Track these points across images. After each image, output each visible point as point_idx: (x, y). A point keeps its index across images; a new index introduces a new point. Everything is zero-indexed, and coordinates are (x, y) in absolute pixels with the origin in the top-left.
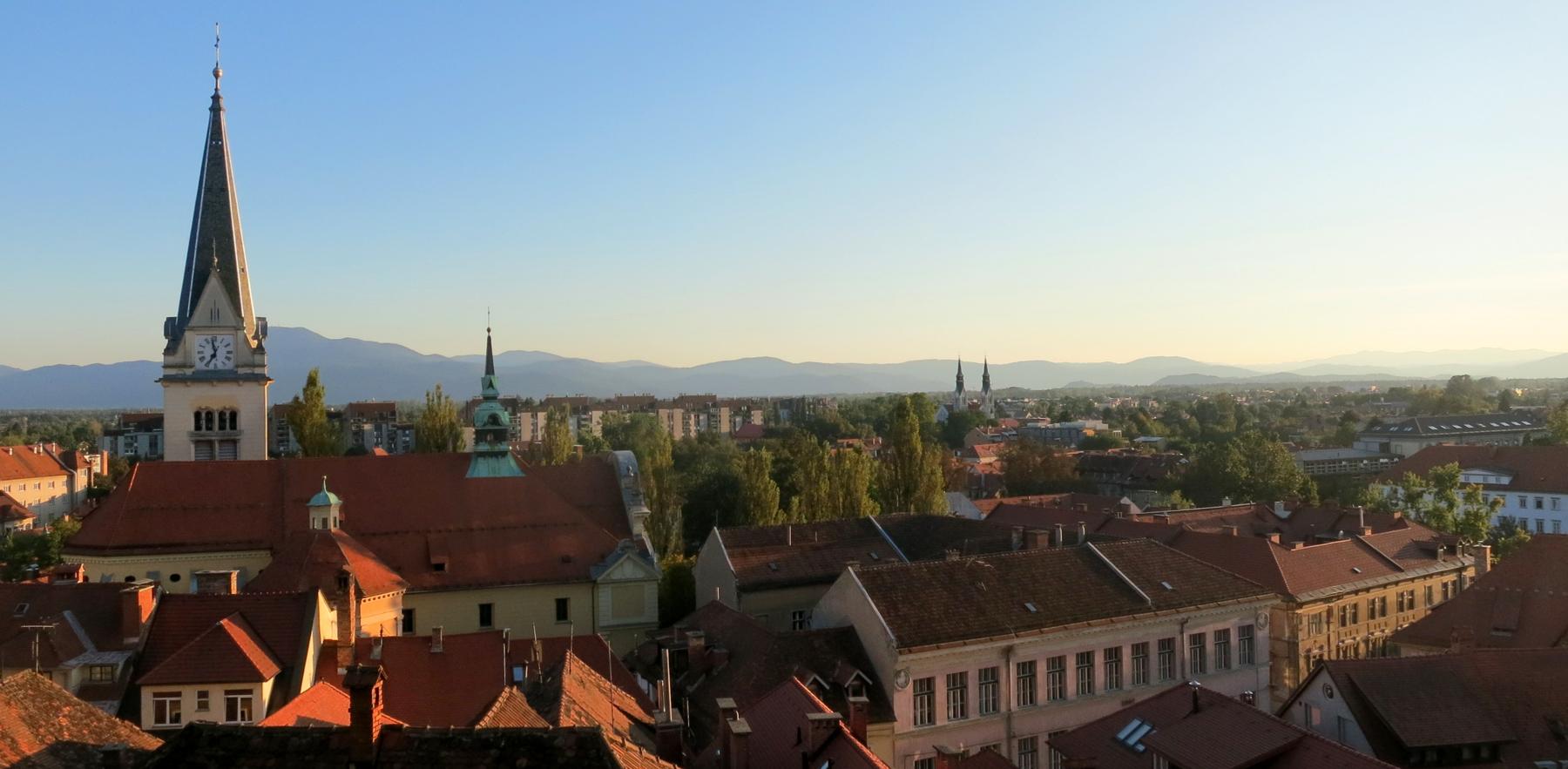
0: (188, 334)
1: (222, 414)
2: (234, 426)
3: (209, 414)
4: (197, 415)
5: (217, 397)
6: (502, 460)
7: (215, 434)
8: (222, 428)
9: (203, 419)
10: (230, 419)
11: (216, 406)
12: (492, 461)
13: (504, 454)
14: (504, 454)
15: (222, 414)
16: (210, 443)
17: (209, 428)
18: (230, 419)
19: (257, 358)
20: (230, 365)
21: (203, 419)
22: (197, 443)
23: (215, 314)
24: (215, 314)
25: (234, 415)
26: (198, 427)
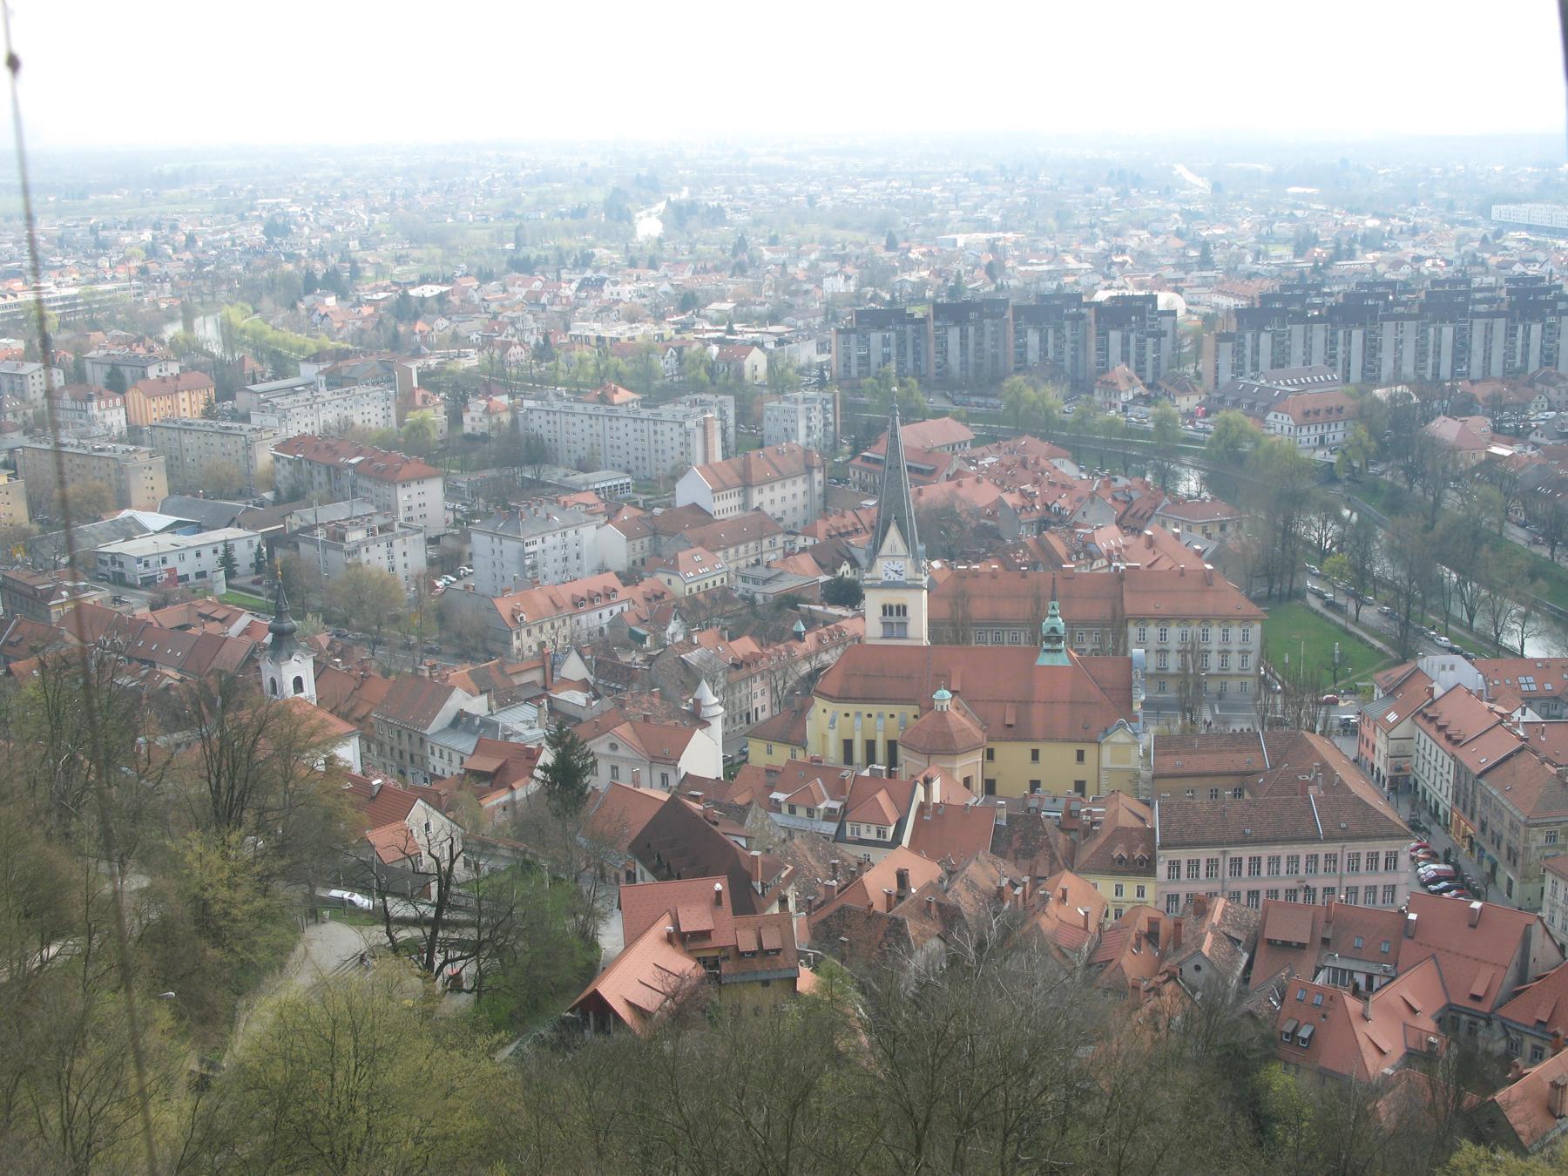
0: (878, 560)
1: (898, 607)
2: (905, 614)
3: (891, 607)
4: (884, 607)
5: (894, 597)
6: (1059, 655)
7: (894, 619)
8: (898, 614)
9: (887, 610)
10: (902, 610)
11: (894, 603)
12: (1052, 655)
13: (1060, 651)
14: (1060, 651)
15: (898, 607)
16: (892, 624)
17: (891, 614)
18: (902, 610)
19: (918, 576)
20: (902, 579)
21: (887, 610)
22: (884, 623)
23: (893, 548)
24: (893, 548)
25: (905, 608)
26: (885, 614)
